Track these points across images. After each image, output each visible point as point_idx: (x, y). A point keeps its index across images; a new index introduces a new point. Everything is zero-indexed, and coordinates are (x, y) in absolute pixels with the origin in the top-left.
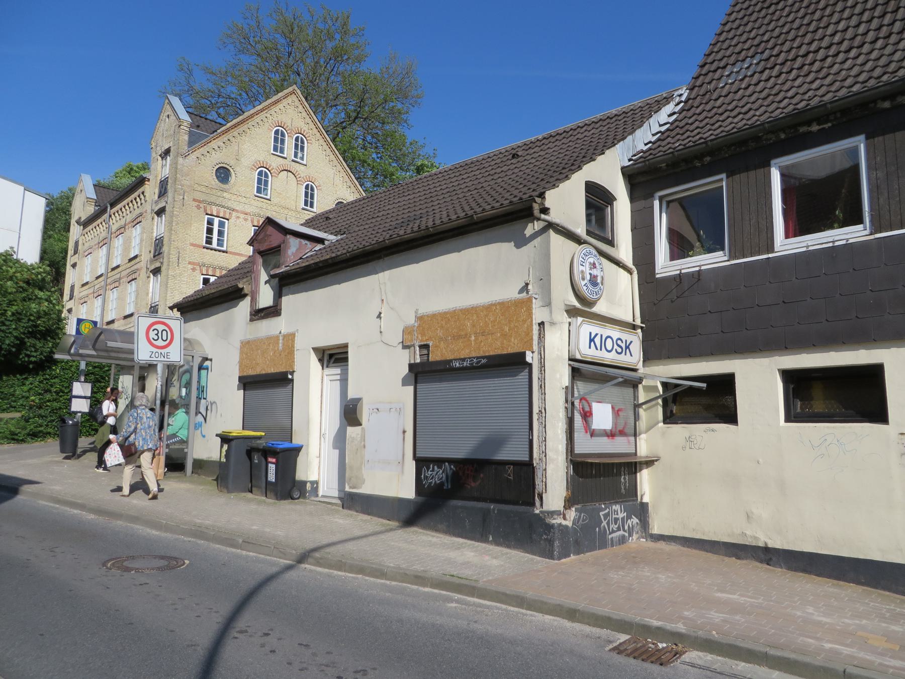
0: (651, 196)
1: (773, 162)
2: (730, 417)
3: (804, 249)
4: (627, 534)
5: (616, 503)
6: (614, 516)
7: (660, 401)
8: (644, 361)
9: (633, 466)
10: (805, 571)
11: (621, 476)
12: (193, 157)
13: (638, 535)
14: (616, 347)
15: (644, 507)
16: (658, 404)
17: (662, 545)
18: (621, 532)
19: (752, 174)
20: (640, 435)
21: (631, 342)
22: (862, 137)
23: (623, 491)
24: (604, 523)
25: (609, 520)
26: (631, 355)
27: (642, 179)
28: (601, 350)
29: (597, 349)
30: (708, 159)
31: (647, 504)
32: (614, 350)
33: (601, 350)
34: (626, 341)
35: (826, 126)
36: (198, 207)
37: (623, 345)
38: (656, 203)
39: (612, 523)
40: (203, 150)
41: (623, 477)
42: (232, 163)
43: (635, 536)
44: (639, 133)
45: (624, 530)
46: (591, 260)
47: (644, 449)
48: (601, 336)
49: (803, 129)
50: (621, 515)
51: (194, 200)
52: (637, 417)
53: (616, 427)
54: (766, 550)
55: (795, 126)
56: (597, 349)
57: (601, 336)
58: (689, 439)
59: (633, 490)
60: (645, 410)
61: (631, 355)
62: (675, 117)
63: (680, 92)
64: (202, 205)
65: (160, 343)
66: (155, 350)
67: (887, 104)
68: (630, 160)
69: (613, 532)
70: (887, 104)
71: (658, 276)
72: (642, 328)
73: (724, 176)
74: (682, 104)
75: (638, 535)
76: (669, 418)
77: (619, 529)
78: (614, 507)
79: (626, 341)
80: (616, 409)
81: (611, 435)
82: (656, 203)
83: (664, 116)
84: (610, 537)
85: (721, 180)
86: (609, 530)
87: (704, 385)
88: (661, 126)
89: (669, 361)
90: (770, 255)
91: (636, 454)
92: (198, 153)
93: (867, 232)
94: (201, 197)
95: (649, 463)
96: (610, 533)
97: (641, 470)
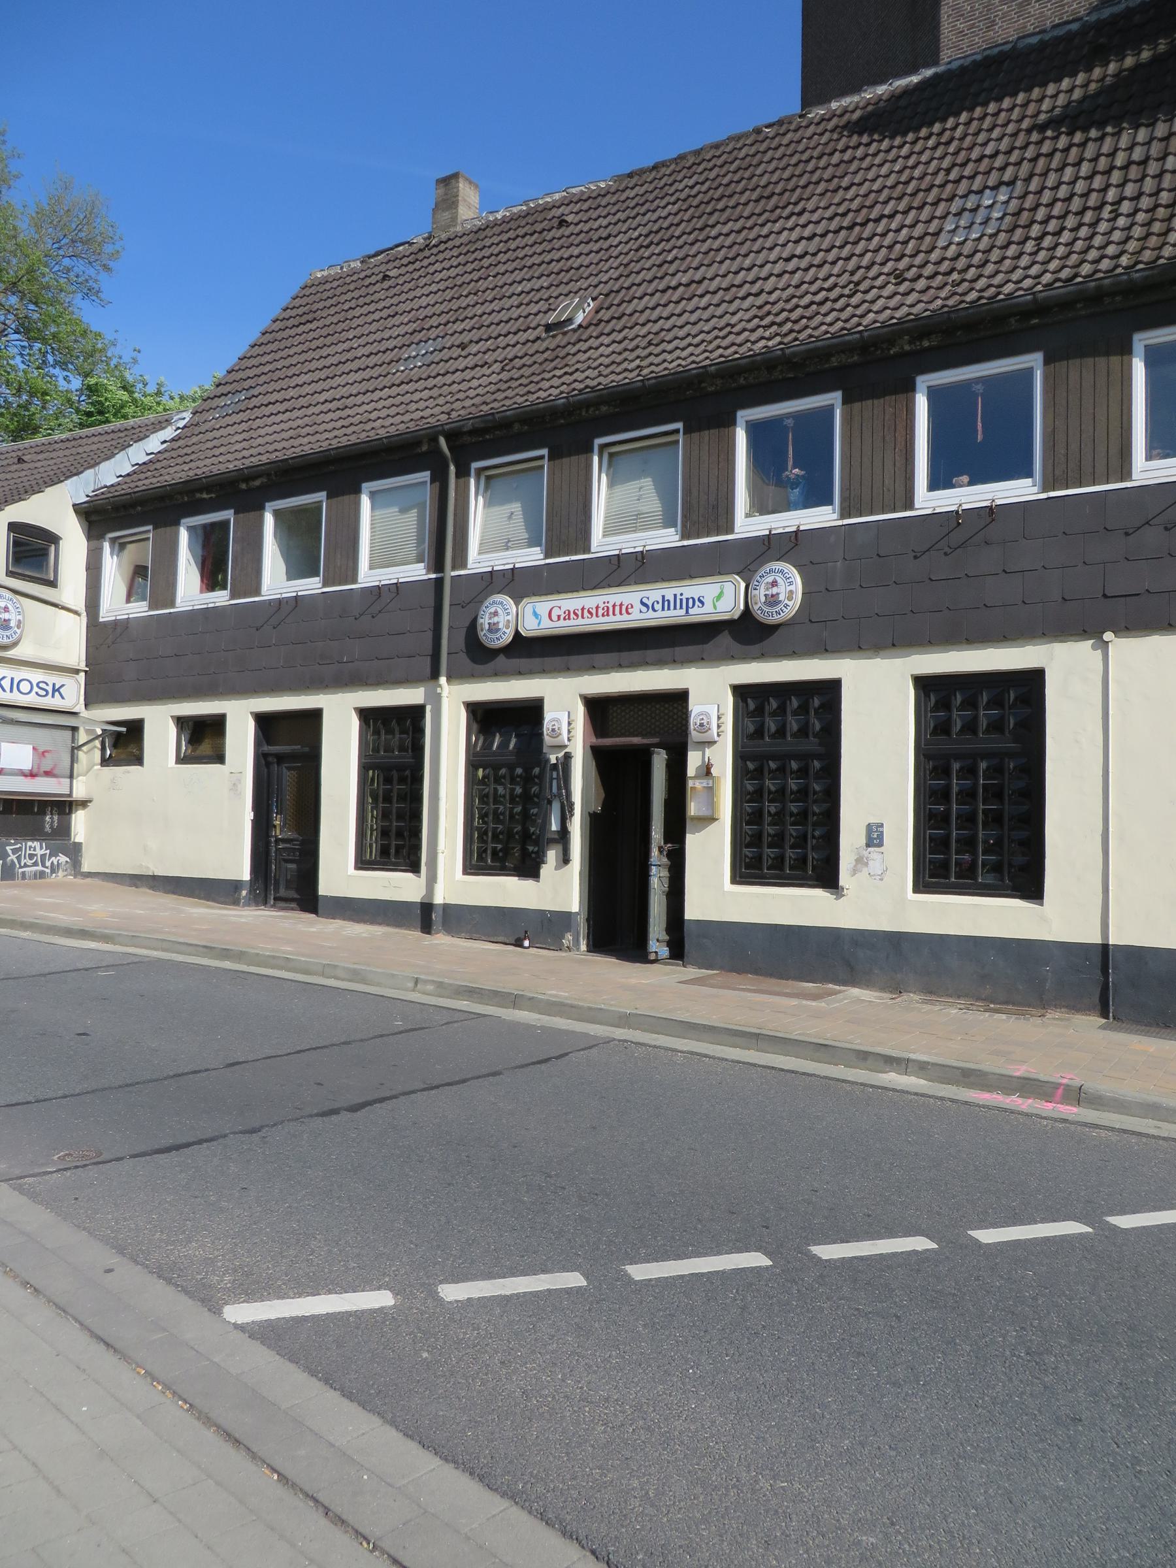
0: (101, 537)
1: (183, 521)
2: (138, 760)
3: (191, 608)
4: (48, 871)
5: (32, 840)
6: (28, 852)
7: (97, 743)
8: (86, 705)
9: (65, 806)
10: (174, 893)
11: (45, 814)
13: (65, 873)
14: (36, 689)
15: (78, 847)
16: (95, 747)
17: (89, 880)
18: (40, 868)
19: (168, 528)
20: (78, 776)
21: (63, 686)
22: (232, 511)
23: (48, 828)
24: (13, 857)
25: (20, 855)
26: (63, 698)
27: (93, 518)
28: (11, 691)
29: (4, 690)
30: (139, 508)
31: (80, 844)
32: (33, 692)
33: (11, 691)
34: (54, 685)
35: (213, 495)
37: (50, 689)
38: (106, 546)
39: (25, 858)
41: (48, 818)
43: (61, 874)
44: (104, 466)
45: (44, 865)
47: (79, 793)
48: (12, 679)
49: (198, 495)
50: (39, 852)
52: (73, 760)
53: (38, 768)
54: (154, 877)
55: (192, 492)
56: (4, 690)
57: (12, 679)
58: (113, 781)
59: (64, 831)
60: (86, 753)
61: (63, 698)
62: (165, 445)
63: (184, 415)
67: (244, 486)
68: (87, 496)
69: (26, 866)
70: (244, 486)
71: (101, 620)
72: (86, 672)
73: (150, 527)
74: (179, 431)
75: (65, 873)
76: (105, 762)
77: (35, 864)
78: (29, 843)
79: (54, 685)
80: (41, 750)
81: (32, 775)
82: (106, 546)
83: (154, 443)
84: (20, 870)
85: (148, 531)
86: (20, 864)
87: (124, 729)
88: (148, 454)
89: (102, 705)
90: (172, 610)
91: (70, 795)
93: (228, 598)
95: (84, 804)
96: (21, 867)
97: (76, 811)
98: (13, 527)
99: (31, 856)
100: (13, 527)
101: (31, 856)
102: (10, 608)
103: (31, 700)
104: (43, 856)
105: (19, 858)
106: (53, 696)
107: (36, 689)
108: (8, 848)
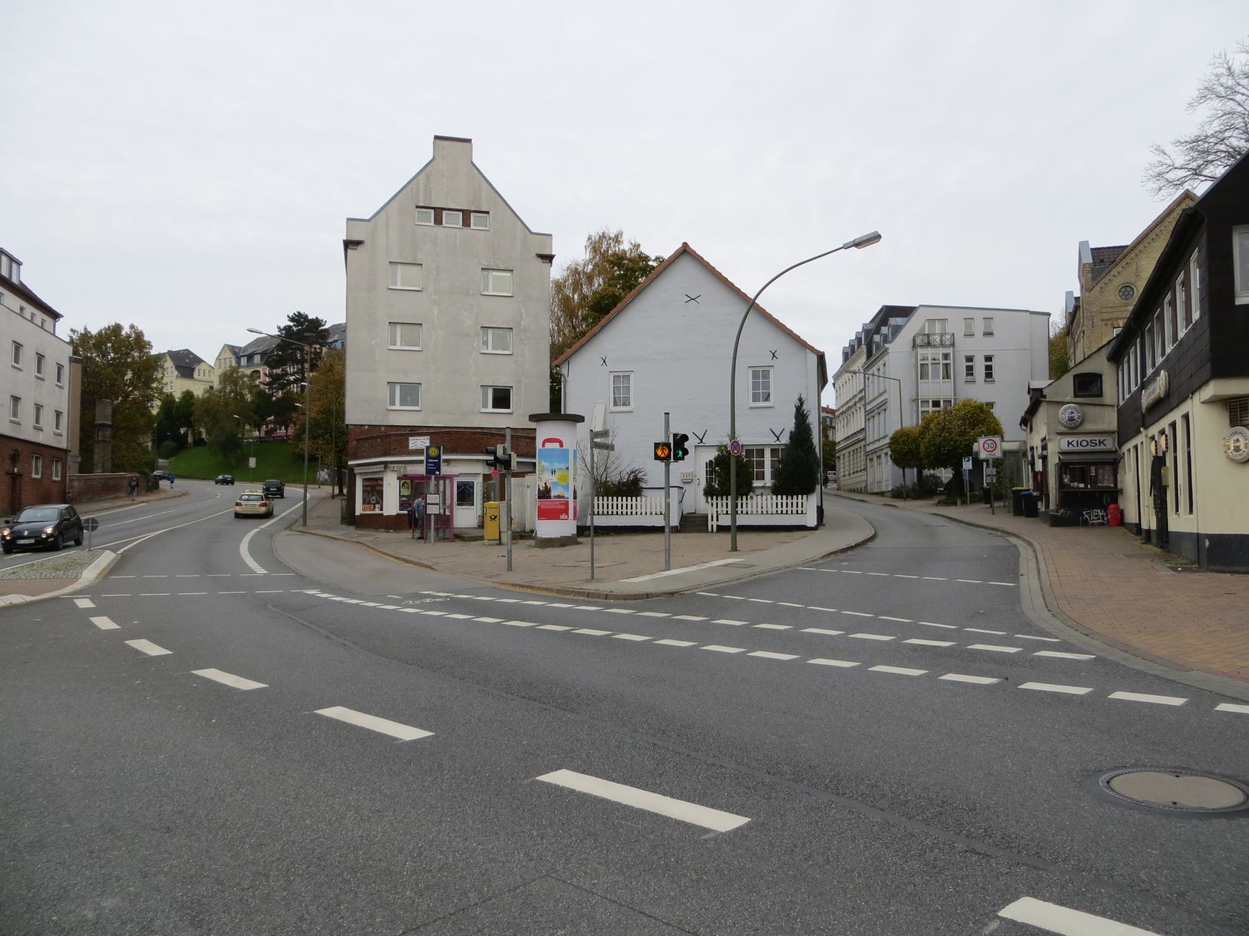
12: (1098, 288)
14: (1090, 443)
18: (1101, 521)
28: (1078, 446)
29: (1073, 446)
33: (1078, 446)
36: (1106, 325)
37: (1097, 442)
40: (1106, 280)
42: (1132, 280)
45: (1103, 519)
46: (1070, 411)
48: (1077, 441)
51: (1102, 320)
56: (1073, 446)
57: (1077, 441)
64: (1109, 323)
65: (990, 449)
66: (988, 453)
69: (1093, 520)
77: (1099, 519)
78: (1095, 510)
79: (1099, 440)
92: (1101, 284)
94: (1106, 316)
98: (1075, 377)
99: (1096, 516)
100: (1075, 377)
101: (1096, 516)
102: (1074, 411)
103: (1089, 448)
104: (1103, 516)
105: (1090, 517)
106: (1100, 445)
107: (1090, 443)
108: (1084, 512)
